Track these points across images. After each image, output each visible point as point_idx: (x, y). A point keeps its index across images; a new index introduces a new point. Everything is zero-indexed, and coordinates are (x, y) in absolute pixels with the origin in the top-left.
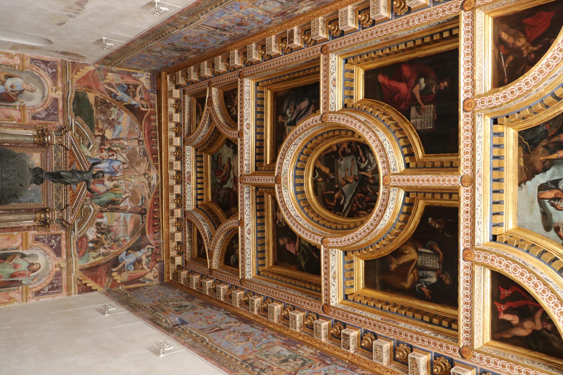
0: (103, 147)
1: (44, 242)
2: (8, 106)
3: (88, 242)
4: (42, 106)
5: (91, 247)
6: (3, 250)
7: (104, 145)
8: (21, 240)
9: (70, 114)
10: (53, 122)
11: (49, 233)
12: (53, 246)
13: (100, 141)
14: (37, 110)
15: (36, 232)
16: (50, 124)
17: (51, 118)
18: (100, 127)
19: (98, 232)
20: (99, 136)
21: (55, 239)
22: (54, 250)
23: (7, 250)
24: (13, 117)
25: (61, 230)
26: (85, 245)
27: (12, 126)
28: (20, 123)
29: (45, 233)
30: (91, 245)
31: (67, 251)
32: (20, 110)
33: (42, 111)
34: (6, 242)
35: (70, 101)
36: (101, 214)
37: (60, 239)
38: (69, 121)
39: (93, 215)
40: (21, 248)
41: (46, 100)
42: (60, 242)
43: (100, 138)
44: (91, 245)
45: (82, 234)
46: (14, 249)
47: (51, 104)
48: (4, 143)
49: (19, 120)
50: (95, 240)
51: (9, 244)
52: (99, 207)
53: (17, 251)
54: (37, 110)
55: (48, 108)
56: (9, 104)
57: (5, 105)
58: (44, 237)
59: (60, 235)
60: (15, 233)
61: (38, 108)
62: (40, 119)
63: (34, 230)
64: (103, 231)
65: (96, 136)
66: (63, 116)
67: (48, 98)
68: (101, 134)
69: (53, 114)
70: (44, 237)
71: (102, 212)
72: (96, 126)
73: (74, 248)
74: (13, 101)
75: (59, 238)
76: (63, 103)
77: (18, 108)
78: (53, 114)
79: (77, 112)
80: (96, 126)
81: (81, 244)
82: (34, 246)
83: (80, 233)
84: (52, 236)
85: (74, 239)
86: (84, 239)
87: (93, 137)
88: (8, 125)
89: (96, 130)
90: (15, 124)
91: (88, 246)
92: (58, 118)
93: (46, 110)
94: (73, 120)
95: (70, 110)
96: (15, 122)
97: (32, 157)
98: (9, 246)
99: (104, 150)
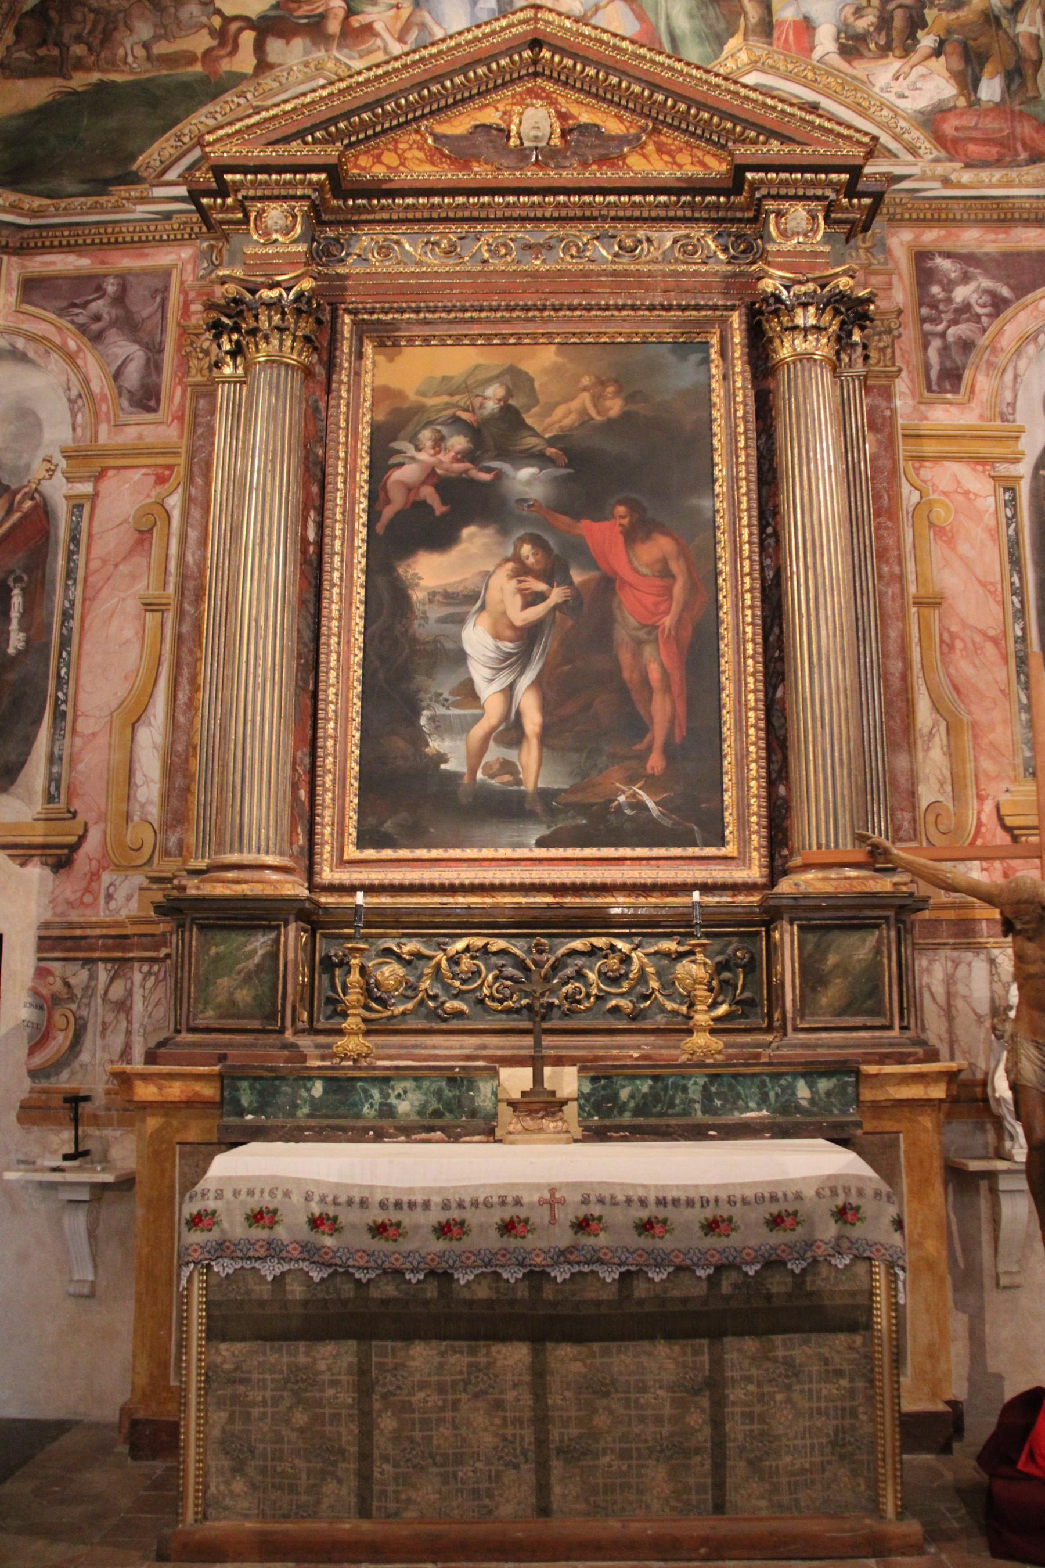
0: (333, 27)
1: (967, 346)
2: (74, 539)
3: (974, 103)
4: (71, 358)
5: (1007, 88)
6: (1016, 562)
7: (323, 17)
8: (955, 467)
9: (118, 208)
10: (174, 297)
11: (908, 318)
12: (993, 294)
13: (298, 43)
14: (99, 383)
15: (902, 385)
16: (186, 313)
17: (144, 310)
18: (202, 42)
19: (907, 52)
20: (259, 47)
21: (949, 287)
22: (1022, 290)
23: (1015, 544)
24: (145, 512)
25: (886, 250)
26: (990, 124)
27: (196, 513)
28: (181, 471)
29: (909, 336)
30: (991, 89)
31: (1027, 222)
32: (99, 476)
33: (103, 360)
34: (963, 548)
35: (33, 213)
36: (785, 34)
37: (948, 255)
38: (168, 216)
39: (788, 77)
40: (1003, 469)
41: (31, 338)
42: (969, 260)
43: (275, 47)
44: (991, 89)
45: (915, 134)
46: (1013, 503)
47: (61, 313)
48: (304, 540)
49: (161, 480)
50: (957, 64)
51: (979, 534)
52: (734, 43)
53: (1024, 489)
54: (96, 387)
55: (83, 329)
56: (62, 532)
57: (70, 555)
58: (936, 344)
59: (921, 257)
60: (909, 496)
61: (87, 382)
62: (153, 366)
63: (888, 394)
64: (899, 21)
65: (263, 66)
66: (139, 244)
67: (19, 333)
68: (248, 37)
69: (120, 300)
70: (936, 344)
71: (767, 28)
72: (198, 68)
73: (1009, 184)
74: (43, 511)
75: (945, 264)
76: (51, 249)
77: (87, 488)
78: (120, 300)
79: (110, 172)
80: (198, 68)
81: (986, 141)
82: (997, 394)
83: (913, 151)
84: (923, 298)
85: (946, 182)
86: (948, 128)
87: (268, 82)
88: (193, 534)
89: (226, 66)
90: (188, 501)
91: (998, 107)
92: (146, 272)
93: (97, 338)
94: (159, 192)
95: (94, 209)
96: (174, 502)
97: (400, 394)
98: (994, 533)
99: (356, 22)
